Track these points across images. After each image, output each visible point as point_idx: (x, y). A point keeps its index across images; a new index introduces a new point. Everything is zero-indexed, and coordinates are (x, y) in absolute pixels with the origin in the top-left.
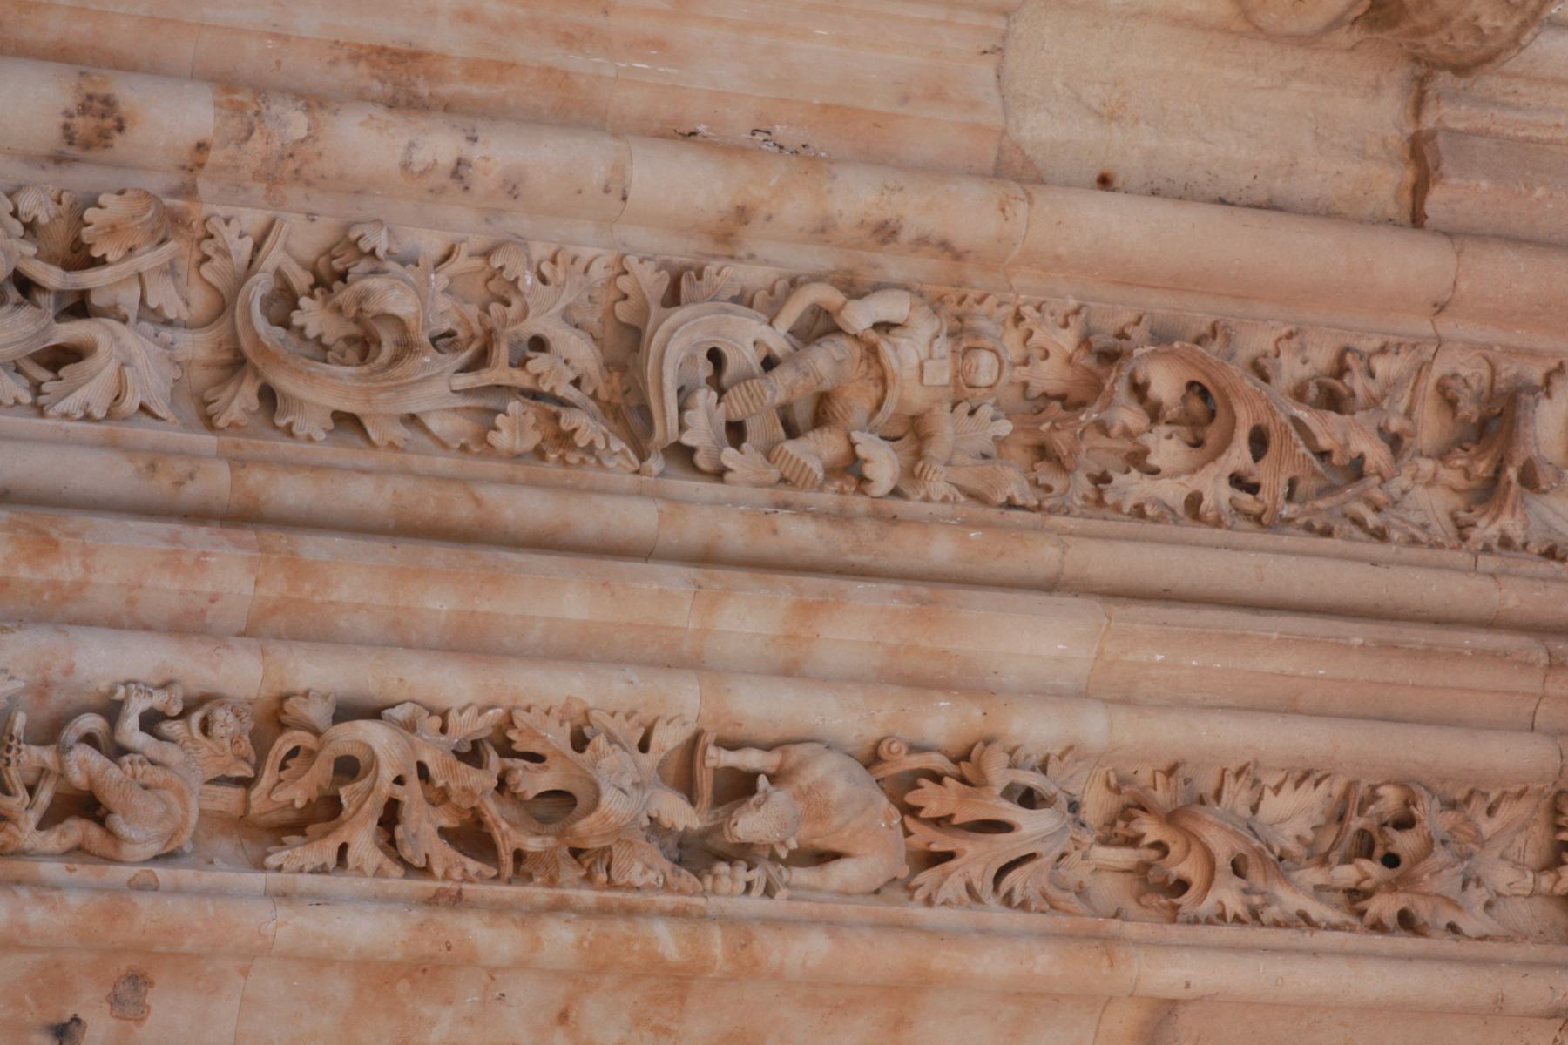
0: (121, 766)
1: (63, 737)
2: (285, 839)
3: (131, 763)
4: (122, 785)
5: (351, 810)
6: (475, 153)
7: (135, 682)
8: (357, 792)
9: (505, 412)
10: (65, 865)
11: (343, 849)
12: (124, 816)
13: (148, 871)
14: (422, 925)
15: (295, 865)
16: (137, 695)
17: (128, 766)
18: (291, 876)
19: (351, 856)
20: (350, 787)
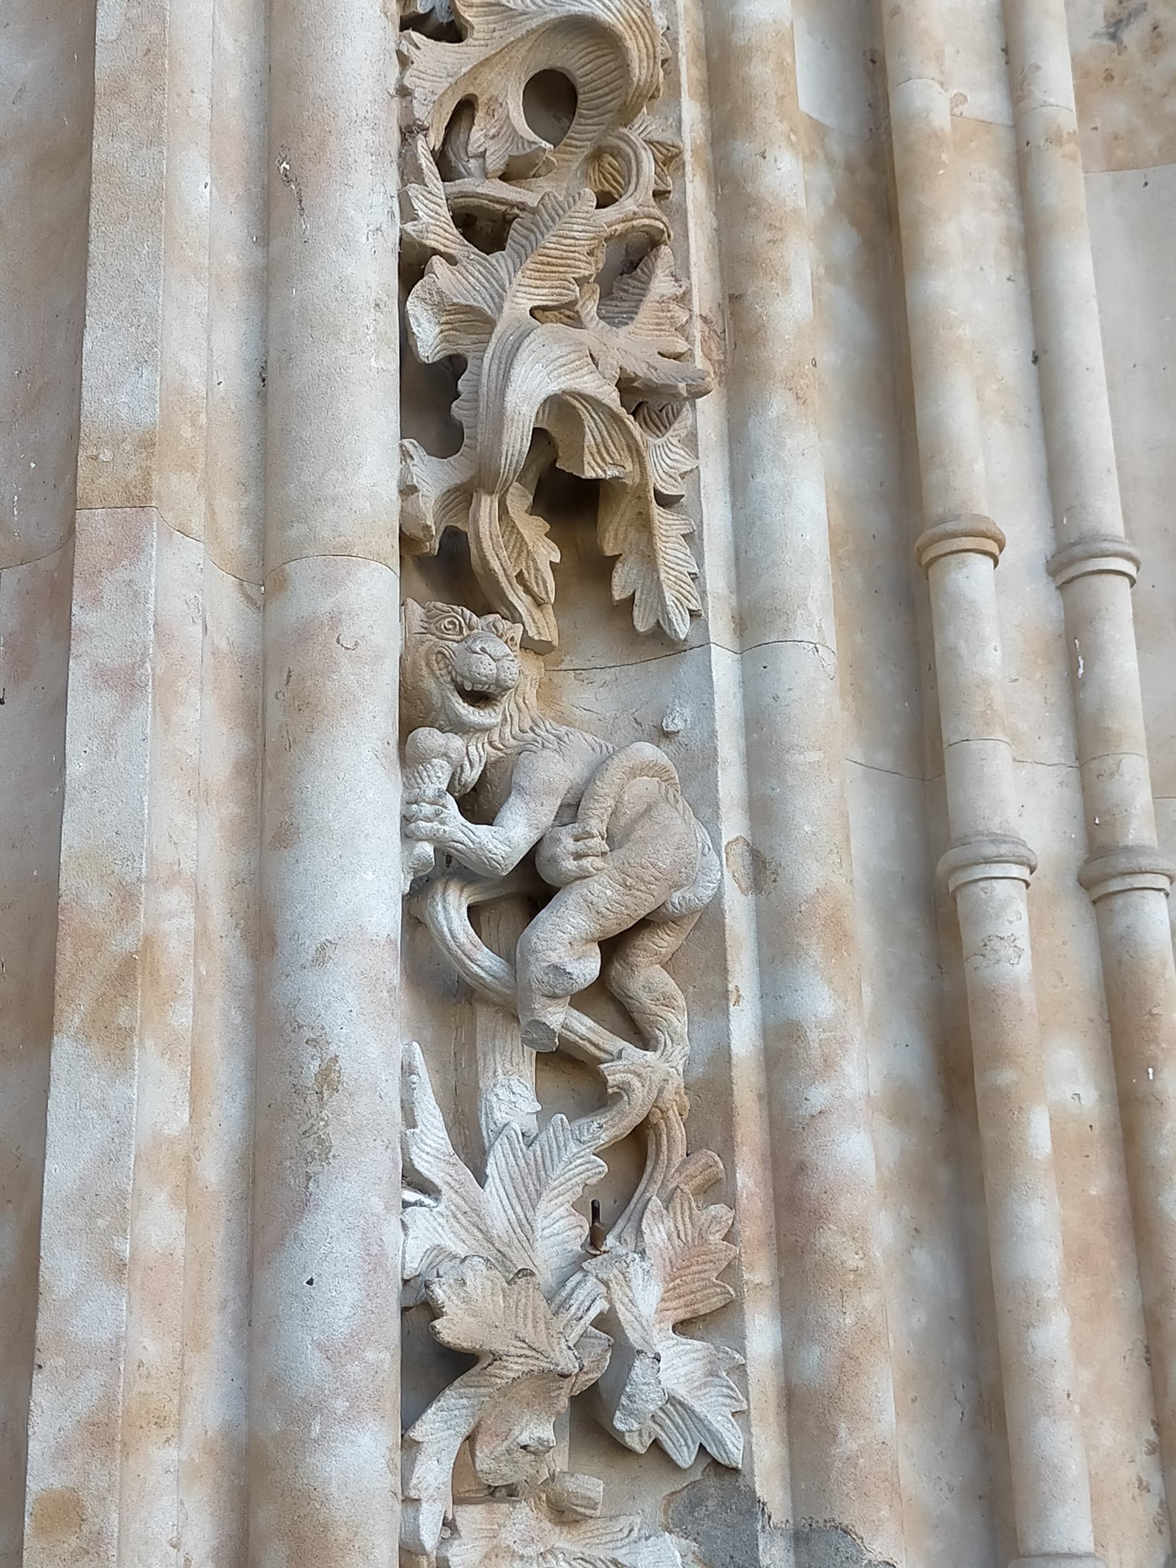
0: (583, 876)
1: (483, 974)
2: (618, 595)
3: (578, 856)
4: (629, 881)
5: (629, 466)
7: (406, 819)
8: (602, 448)
10: (731, 1004)
12: (677, 886)
13: (727, 853)
14: (798, 398)
15: (691, 587)
16: (443, 823)
17: (586, 862)
18: (710, 599)
19: (669, 490)
20: (587, 457)
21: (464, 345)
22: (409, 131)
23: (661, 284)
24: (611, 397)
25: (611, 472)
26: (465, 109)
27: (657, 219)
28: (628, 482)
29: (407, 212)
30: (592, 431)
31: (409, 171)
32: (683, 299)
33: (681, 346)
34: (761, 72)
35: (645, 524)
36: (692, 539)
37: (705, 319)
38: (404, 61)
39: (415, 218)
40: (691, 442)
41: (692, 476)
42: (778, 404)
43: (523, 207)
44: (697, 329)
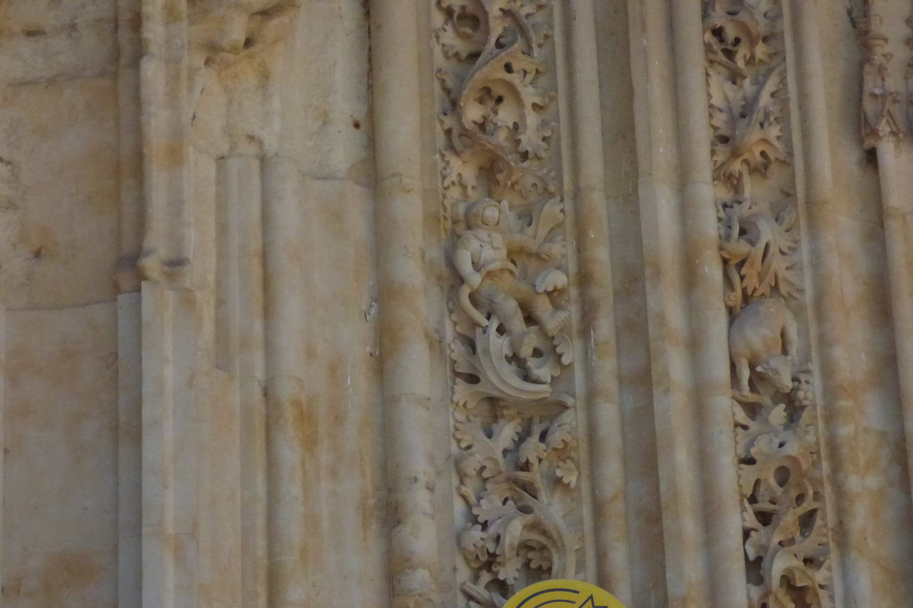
6: (423, 479)
9: (562, 478)
11: (821, 587)
21: (761, 554)
22: (742, 496)
23: (818, 522)
24: (802, 564)
25: (804, 585)
26: (758, 483)
27: (815, 505)
28: (810, 586)
29: (744, 520)
30: (798, 575)
31: (744, 510)
32: (825, 526)
33: (825, 540)
34: (845, 451)
35: (816, 595)
36: (832, 598)
37: (832, 530)
38: (739, 477)
39: (746, 520)
40: (829, 569)
41: (831, 579)
42: (854, 554)
43: (775, 510)
44: (830, 534)
